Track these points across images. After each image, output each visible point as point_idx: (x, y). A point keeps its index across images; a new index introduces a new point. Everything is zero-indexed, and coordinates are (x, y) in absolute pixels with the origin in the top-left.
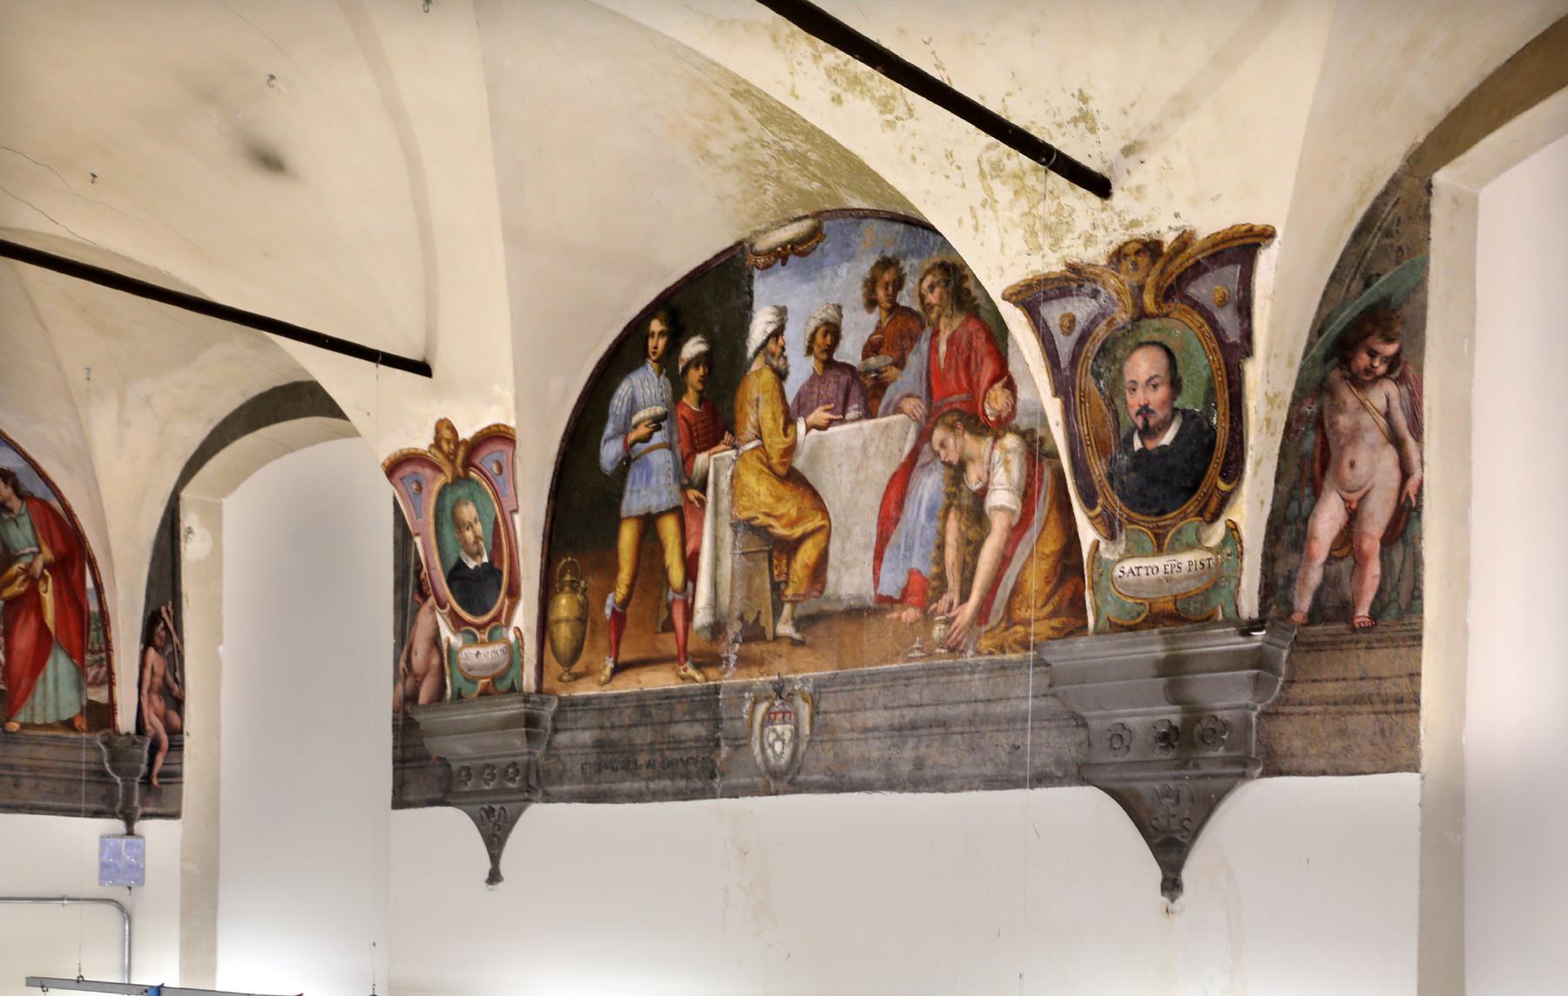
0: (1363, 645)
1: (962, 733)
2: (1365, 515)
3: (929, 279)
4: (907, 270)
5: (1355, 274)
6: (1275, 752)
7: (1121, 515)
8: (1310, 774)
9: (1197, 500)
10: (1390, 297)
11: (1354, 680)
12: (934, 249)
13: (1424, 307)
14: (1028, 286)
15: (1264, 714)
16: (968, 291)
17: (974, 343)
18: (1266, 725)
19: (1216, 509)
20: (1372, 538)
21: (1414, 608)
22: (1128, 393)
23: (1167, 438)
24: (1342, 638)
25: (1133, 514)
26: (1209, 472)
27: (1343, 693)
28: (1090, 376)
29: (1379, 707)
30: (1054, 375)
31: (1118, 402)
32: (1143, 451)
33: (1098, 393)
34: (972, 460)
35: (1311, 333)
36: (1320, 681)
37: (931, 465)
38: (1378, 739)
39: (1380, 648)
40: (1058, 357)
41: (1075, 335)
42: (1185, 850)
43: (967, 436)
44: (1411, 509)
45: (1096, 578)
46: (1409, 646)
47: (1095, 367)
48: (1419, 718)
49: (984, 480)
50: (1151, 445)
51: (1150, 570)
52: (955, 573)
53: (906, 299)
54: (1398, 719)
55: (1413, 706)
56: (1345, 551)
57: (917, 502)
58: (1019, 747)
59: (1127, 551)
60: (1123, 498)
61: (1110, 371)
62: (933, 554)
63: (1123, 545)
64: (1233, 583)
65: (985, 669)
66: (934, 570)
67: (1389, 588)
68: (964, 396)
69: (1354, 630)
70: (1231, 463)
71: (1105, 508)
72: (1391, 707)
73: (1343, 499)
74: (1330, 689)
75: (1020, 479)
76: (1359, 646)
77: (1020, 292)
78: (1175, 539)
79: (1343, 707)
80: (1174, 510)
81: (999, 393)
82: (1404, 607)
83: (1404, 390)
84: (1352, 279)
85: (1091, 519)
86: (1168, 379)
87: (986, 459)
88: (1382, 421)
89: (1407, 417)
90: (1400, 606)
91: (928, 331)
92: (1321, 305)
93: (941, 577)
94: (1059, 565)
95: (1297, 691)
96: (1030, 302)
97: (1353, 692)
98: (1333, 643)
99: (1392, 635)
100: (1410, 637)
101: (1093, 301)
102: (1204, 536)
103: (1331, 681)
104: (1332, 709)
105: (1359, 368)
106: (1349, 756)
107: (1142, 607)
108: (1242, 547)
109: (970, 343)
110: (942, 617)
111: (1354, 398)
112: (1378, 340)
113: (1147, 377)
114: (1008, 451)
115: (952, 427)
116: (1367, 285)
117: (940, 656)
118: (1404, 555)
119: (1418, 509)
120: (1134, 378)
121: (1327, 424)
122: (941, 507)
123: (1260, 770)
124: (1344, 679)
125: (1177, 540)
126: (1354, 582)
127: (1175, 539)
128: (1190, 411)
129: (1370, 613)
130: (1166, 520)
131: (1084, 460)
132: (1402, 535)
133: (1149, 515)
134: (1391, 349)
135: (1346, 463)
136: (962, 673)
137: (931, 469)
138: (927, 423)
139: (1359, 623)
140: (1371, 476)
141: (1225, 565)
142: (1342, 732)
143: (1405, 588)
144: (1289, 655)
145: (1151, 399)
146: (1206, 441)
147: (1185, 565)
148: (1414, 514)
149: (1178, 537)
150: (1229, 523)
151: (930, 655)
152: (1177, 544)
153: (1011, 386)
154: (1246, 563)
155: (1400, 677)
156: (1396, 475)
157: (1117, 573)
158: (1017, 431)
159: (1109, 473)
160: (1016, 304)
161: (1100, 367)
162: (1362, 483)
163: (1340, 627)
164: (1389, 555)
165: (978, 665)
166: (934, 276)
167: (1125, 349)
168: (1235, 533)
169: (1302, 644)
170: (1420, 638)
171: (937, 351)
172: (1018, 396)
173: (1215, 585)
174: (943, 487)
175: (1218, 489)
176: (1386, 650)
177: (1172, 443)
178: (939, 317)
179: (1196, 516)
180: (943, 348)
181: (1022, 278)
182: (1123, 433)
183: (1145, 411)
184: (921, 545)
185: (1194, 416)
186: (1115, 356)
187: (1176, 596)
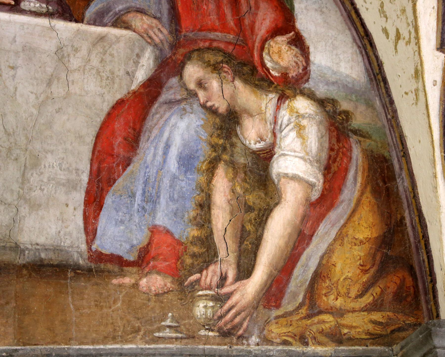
57: (162, 145)
62: (192, 214)
66: (195, 232)
117: (207, 340)
151: (192, 337)
184: (172, 199)
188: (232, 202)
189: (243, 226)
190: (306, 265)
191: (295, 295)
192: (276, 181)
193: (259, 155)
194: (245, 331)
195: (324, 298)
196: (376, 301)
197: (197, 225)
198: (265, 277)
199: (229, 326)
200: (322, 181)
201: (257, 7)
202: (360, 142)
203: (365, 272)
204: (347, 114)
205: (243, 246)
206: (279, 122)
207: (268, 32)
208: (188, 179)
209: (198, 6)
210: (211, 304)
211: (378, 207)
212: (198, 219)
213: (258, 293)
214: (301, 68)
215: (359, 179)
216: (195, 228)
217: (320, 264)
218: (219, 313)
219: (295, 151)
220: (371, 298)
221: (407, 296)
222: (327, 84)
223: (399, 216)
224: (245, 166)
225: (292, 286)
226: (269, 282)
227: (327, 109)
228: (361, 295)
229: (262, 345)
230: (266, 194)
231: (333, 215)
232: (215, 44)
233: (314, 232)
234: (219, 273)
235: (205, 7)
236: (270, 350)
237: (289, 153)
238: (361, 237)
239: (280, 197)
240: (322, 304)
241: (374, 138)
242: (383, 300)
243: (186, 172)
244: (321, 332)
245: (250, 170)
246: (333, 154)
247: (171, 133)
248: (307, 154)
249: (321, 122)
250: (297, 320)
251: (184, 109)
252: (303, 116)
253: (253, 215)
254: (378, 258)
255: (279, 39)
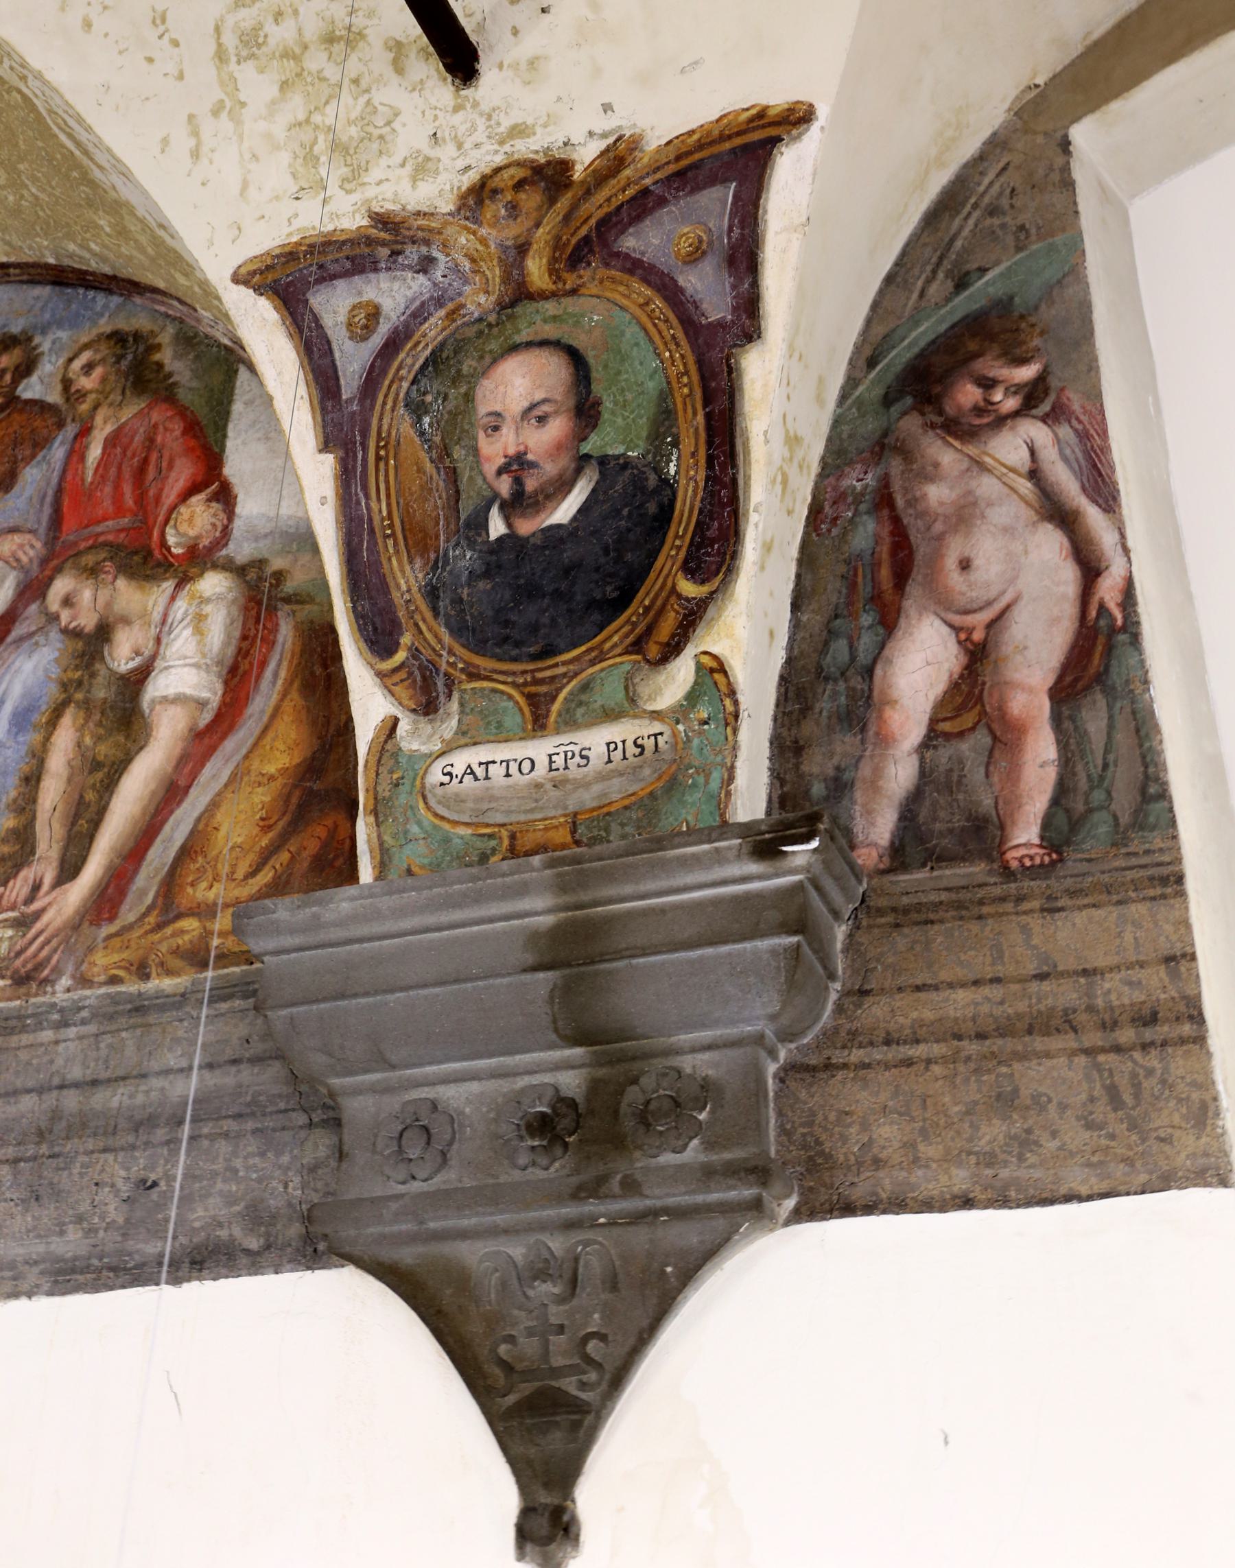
0: (1035, 904)
1: (16, 1161)
2: (1007, 649)
3: (85, 357)
4: (46, 347)
5: (934, 272)
6: (828, 1157)
7: (453, 665)
8: (928, 1206)
9: (628, 621)
10: (1011, 298)
11: (1023, 980)
12: (102, 315)
13: (1085, 309)
14: (290, 255)
15: (791, 1070)
16: (160, 366)
17: (159, 439)
18: (803, 1095)
19: (673, 636)
20: (1031, 690)
21: (1152, 819)
22: (481, 435)
23: (564, 512)
24: (981, 893)
25: (479, 661)
26: (658, 564)
27: (998, 1011)
28: (401, 411)
29: (1094, 1038)
30: (324, 410)
31: (458, 453)
32: (510, 540)
33: (417, 439)
34: (126, 621)
35: (851, 362)
36: (936, 988)
37: (40, 638)
38: (1101, 1110)
39: (1080, 908)
40: (337, 379)
41: (377, 339)
42: (589, 1419)
43: (121, 583)
44: (1113, 630)
45: (384, 789)
46: (1153, 899)
47: (414, 394)
48: (1209, 1055)
49: (147, 653)
50: (526, 527)
51: (514, 768)
52: (56, 826)
53: (31, 389)
54: (1152, 1060)
55: (1187, 1029)
56: (969, 719)
58: (155, 1184)
59: (461, 732)
60: (459, 630)
61: (445, 399)
62: (13, 794)
63: (454, 723)
64: (716, 776)
65: (94, 1016)
67: (1083, 784)
68: (125, 521)
69: (1008, 873)
70: (712, 542)
71: (415, 653)
72: (1126, 1035)
73: (951, 626)
74: (960, 1004)
75: (226, 644)
76: (1026, 906)
77: (268, 268)
78: (576, 700)
79: (1000, 1042)
80: (575, 646)
81: (199, 509)
82: (1125, 819)
83: (1065, 431)
84: (929, 281)
85: (380, 675)
86: (571, 403)
87: (156, 616)
88: (1025, 486)
89: (1079, 474)
90: (1116, 818)
91: (71, 430)
92: (869, 322)
93: (24, 839)
94: (297, 793)
95: (876, 1012)
96: (289, 284)
97: (1022, 1006)
98: (960, 906)
99: (1106, 878)
100: (1151, 879)
101: (421, 278)
102: (644, 690)
103: (963, 985)
104: (972, 1048)
105: (959, 408)
106: (1031, 1158)
107: (493, 843)
108: (736, 703)
109: (151, 440)
110: (11, 914)
111: (958, 456)
112: (996, 363)
113: (526, 404)
114: (205, 601)
115: (93, 572)
116: (961, 284)
118: (1111, 717)
119: (1131, 629)
120: (498, 408)
121: (900, 502)
122: (45, 706)
123: (790, 1203)
124: (997, 980)
125: (580, 704)
126: (995, 779)
127: (576, 700)
128: (617, 457)
129: (1042, 838)
130: (556, 665)
131: (376, 565)
132: (1101, 678)
133: (514, 660)
134: (1026, 373)
135: (951, 562)
136: (39, 1027)
137: (37, 644)
138: (42, 571)
139: (1020, 860)
140: (1013, 581)
141: (696, 742)
142: (1006, 1102)
143: (1123, 781)
144: (850, 936)
145: (531, 444)
146: (652, 508)
147: (598, 751)
148: (1122, 637)
149: (584, 697)
150: (705, 660)
152: (580, 711)
153: (225, 496)
154: (744, 735)
155: (1142, 965)
156: (1068, 576)
157: (436, 775)
158: (228, 566)
159: (429, 584)
160: (259, 290)
161: (425, 394)
162: (993, 593)
163: (977, 870)
164: (1072, 719)
165: (80, 1009)
166: (97, 351)
167: (481, 357)
168: (718, 677)
169: (880, 912)
170: (1180, 879)
171: (82, 459)
172: (238, 510)
173: (672, 785)
174: (55, 672)
175: (679, 596)
176: (1093, 911)
177: (574, 519)
178: (96, 407)
179: (626, 652)
180: (95, 452)
181: (278, 242)
182: (466, 508)
183: (517, 464)
185: (625, 464)
186: (459, 371)
187: (575, 814)
188: (73, 763)
189: (81, 797)
190: (170, 839)
191: (143, 893)
192: (147, 711)
193: (128, 679)
194: (53, 970)
195: (190, 890)
196: (279, 878)
197: (15, 811)
198: (100, 873)
199: (29, 966)
200: (220, 693)
201: (171, 466)
202: (294, 612)
203: (266, 829)
204: (279, 576)
205: (76, 828)
206: (170, 620)
207: (179, 496)
208: (18, 743)
209: (90, 495)
210: (10, 933)
211: (309, 711)
212: (20, 801)
213: (85, 902)
214: (219, 529)
215: (283, 674)
216: (12, 815)
217: (192, 832)
218: (18, 947)
219: (186, 658)
220: (271, 874)
221: (336, 857)
222: (257, 539)
223: (343, 718)
224: (105, 701)
225: (140, 880)
226: (106, 880)
227: (248, 578)
228: (253, 874)
229: (75, 990)
230: (127, 737)
231: (229, 745)
232: (101, 539)
233: (193, 780)
234: (31, 882)
235: (99, 494)
236: (86, 998)
237: (177, 663)
238: (271, 769)
239: (148, 736)
240: (184, 901)
241: (318, 600)
242: (291, 874)
243: (17, 734)
244: (176, 952)
245: (112, 708)
246: (245, 644)
247: (10, 682)
248: (204, 655)
249: (234, 601)
250: (139, 937)
251: (37, 644)
252: (208, 601)
253: (99, 775)
254: (294, 800)
255: (194, 500)
